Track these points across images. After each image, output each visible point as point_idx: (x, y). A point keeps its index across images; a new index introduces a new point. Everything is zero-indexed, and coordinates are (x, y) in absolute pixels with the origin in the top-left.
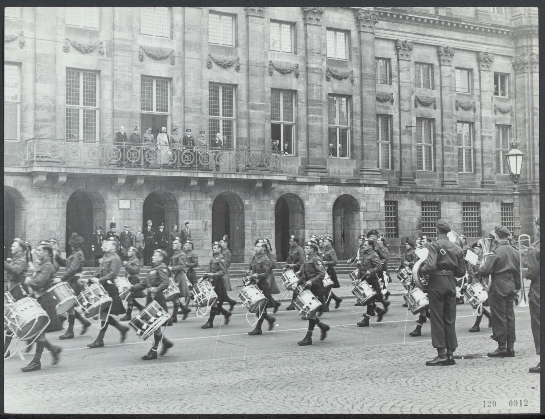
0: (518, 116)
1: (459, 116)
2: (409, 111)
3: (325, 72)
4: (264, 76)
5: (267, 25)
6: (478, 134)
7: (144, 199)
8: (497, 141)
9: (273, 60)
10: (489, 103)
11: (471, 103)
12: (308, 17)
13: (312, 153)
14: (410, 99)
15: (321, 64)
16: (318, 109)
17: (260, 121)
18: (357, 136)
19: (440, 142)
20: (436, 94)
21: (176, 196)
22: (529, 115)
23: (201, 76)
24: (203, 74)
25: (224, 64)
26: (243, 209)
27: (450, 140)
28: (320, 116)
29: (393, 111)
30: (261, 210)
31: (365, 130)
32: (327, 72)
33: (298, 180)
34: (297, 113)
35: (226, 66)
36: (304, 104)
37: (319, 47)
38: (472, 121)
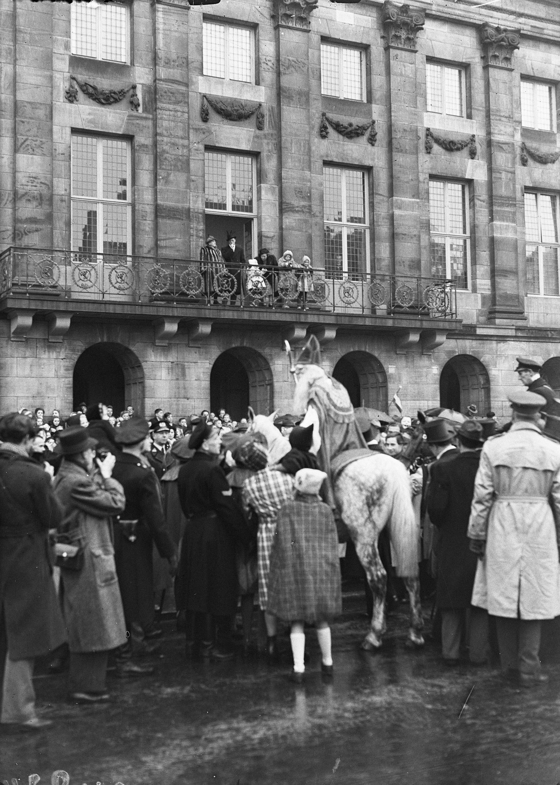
3: (518, 151)
4: (417, 153)
5: (421, 66)
7: (213, 363)
9: (431, 126)
12: (490, 54)
13: (500, 286)
15: (513, 136)
16: (509, 212)
21: (269, 357)
23: (310, 149)
24: (313, 148)
25: (350, 129)
26: (385, 381)
28: (514, 225)
30: (416, 383)
32: (522, 149)
33: (479, 331)
34: (474, 219)
35: (351, 133)
36: (484, 204)
37: (509, 106)
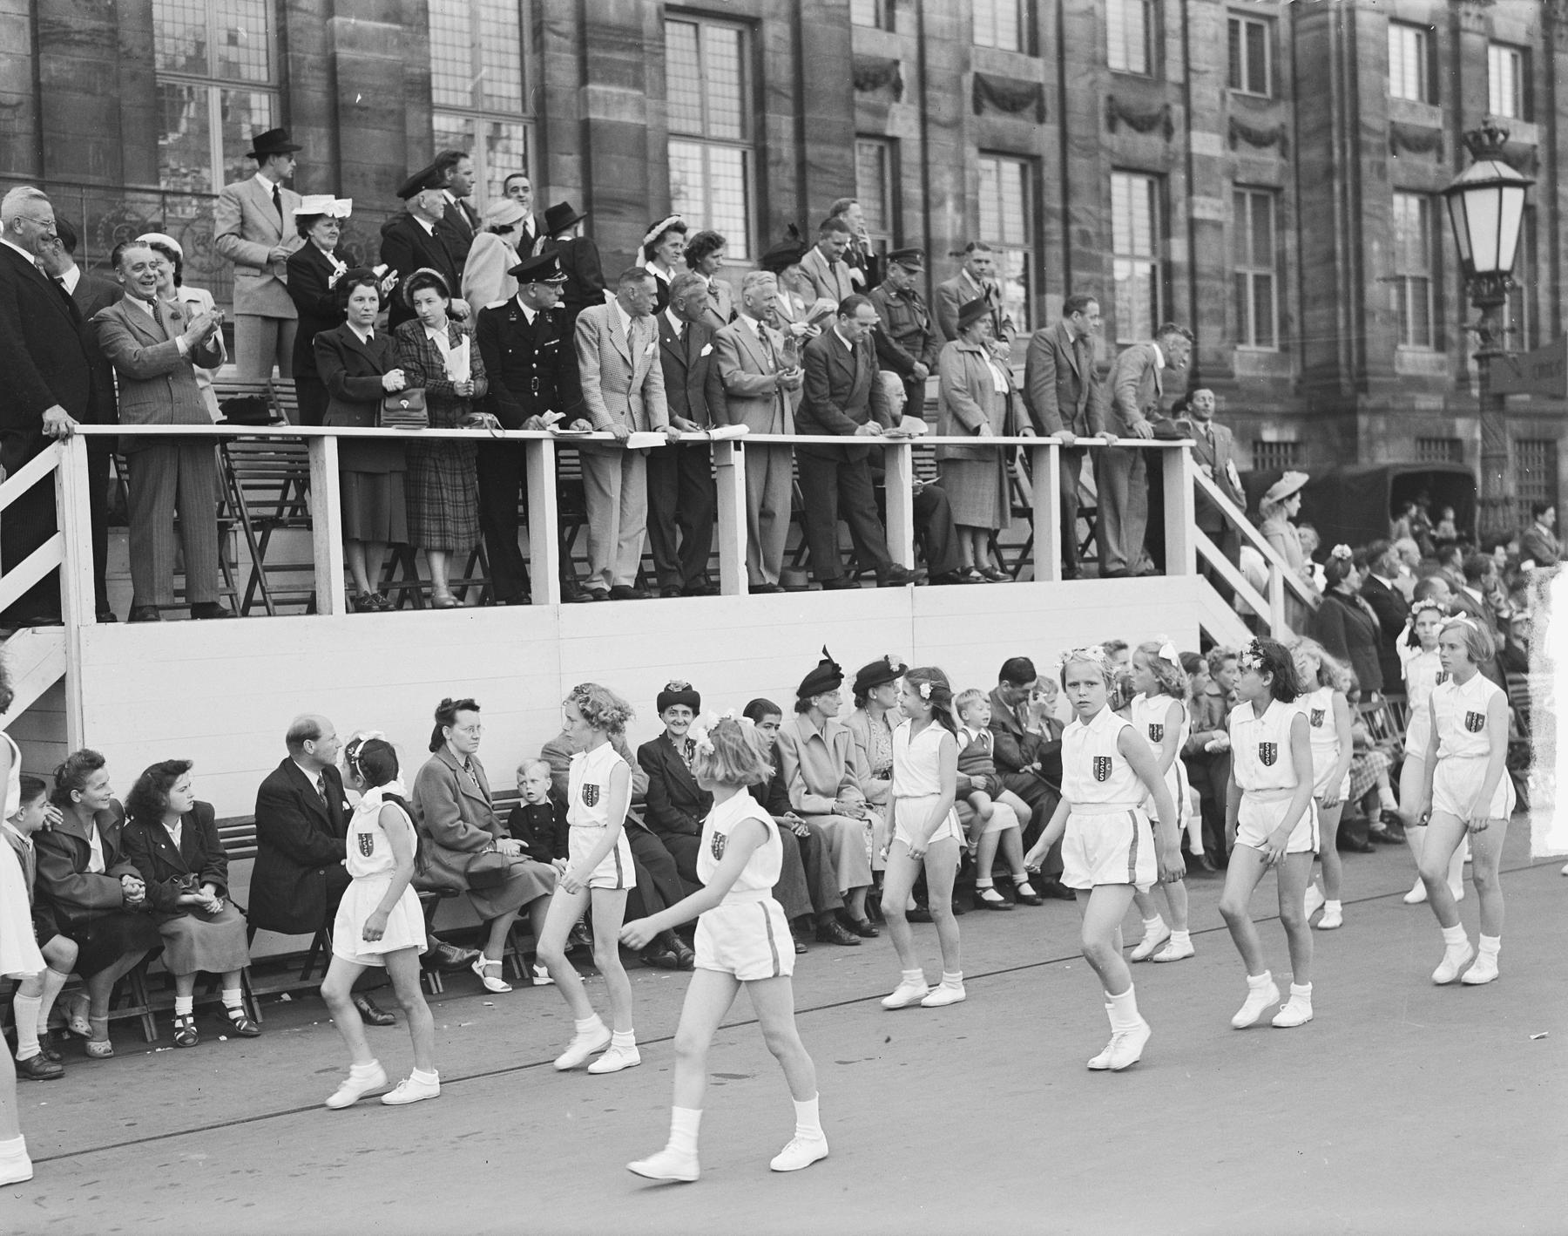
0: (1303, 156)
1: (1116, 149)
2: (955, 124)
6: (1180, 214)
8: (1238, 239)
10: (1212, 110)
11: (1155, 110)
14: (958, 89)
16: (627, 64)
17: (381, 98)
18: (782, 177)
19: (1058, 237)
20: (1040, 71)
22: (1343, 153)
27: (1091, 230)
29: (902, 122)
31: (812, 151)
38: (1159, 168)
